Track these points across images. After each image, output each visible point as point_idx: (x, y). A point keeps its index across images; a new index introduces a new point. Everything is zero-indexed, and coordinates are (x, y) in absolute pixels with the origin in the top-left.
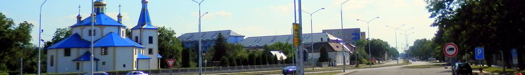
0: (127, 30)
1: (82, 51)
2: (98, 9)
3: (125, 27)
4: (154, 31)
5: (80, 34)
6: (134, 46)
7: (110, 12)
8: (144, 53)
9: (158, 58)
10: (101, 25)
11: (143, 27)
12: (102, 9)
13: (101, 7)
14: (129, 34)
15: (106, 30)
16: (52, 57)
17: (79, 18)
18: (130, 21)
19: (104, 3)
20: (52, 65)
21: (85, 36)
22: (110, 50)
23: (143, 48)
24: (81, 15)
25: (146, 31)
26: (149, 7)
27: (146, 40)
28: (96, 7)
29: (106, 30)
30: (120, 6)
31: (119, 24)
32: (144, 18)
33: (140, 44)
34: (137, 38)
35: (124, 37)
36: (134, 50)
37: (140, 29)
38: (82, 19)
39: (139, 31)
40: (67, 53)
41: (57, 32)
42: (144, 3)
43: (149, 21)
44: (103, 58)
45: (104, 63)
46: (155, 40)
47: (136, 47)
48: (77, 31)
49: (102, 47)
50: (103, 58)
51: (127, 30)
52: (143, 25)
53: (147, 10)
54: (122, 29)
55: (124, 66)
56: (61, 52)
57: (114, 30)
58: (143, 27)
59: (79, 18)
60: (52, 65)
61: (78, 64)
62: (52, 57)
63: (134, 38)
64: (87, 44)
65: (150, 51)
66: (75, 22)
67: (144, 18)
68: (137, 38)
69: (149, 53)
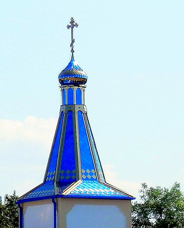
4: (113, 209)
11: (68, 191)
25: (79, 208)
26: (92, 101)
32: (70, 150)
37: (54, 198)
39: (49, 207)
42: (71, 80)
52: (65, 183)
53: (83, 115)
58: (68, 191)
67: (70, 150)
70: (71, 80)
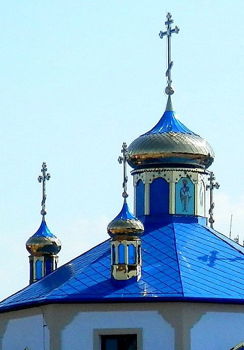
2: (160, 190)
10: (174, 302)
12: (187, 187)
13: (174, 176)
17: (42, 249)
19: (200, 146)
24: (58, 233)
28: (147, 176)
38: (62, 259)
59: (42, 249)
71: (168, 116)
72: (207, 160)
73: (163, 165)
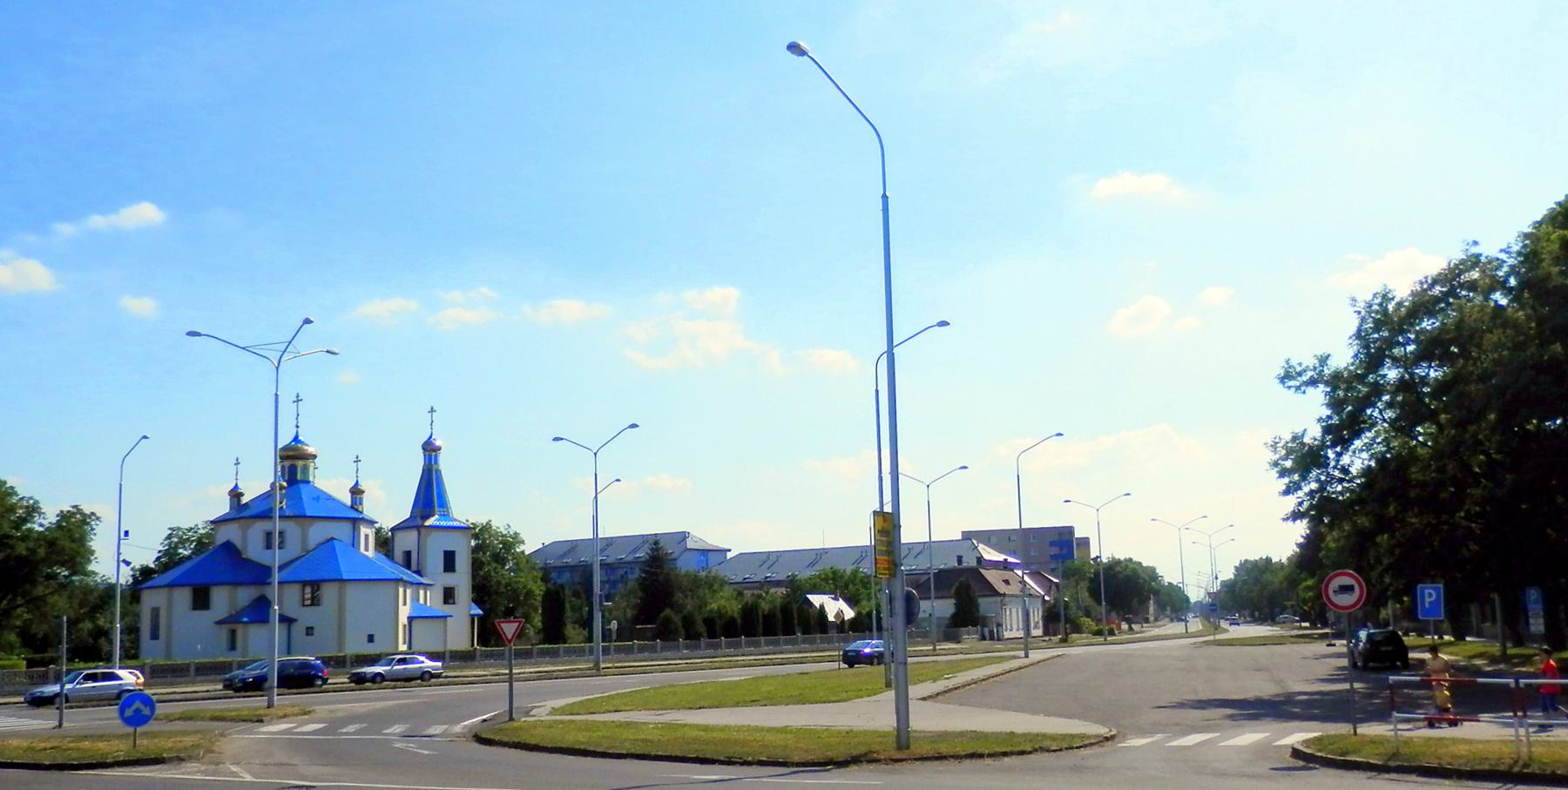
0: (378, 531)
1: (245, 595)
2: (293, 469)
3: (372, 523)
5: (238, 543)
6: (398, 581)
7: (329, 479)
8: (431, 600)
9: (473, 617)
11: (428, 523)
12: (305, 469)
13: (300, 463)
14: (384, 543)
15: (318, 533)
16: (155, 613)
17: (235, 494)
18: (389, 505)
19: (311, 450)
20: (155, 636)
21: (254, 550)
22: (328, 593)
23: (426, 586)
24: (242, 488)
25: (435, 534)
27: (435, 561)
28: (287, 463)
29: (318, 533)
30: (357, 461)
31: (355, 515)
32: (429, 495)
33: (418, 572)
34: (408, 554)
35: (371, 553)
36: (401, 590)
37: (418, 528)
38: (245, 500)
39: (413, 534)
40: (201, 600)
41: (169, 537)
43: (443, 504)
44: (306, 616)
45: (310, 631)
46: (463, 563)
47: (406, 583)
48: (231, 533)
49: (304, 583)
50: (306, 616)
51: (378, 531)
53: (438, 472)
54: (364, 530)
55: (371, 639)
56: (183, 596)
57: (341, 531)
58: (428, 523)
59: (235, 494)
60: (155, 636)
61: (233, 633)
62: (155, 613)
63: (399, 555)
64: (261, 574)
65: (449, 595)
66: (223, 507)
68: (408, 554)
69: (446, 602)
70: (430, 449)
71: (296, 439)
72: (315, 457)
73: (293, 461)
